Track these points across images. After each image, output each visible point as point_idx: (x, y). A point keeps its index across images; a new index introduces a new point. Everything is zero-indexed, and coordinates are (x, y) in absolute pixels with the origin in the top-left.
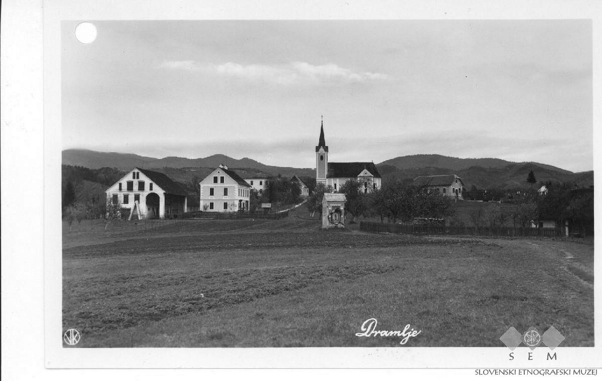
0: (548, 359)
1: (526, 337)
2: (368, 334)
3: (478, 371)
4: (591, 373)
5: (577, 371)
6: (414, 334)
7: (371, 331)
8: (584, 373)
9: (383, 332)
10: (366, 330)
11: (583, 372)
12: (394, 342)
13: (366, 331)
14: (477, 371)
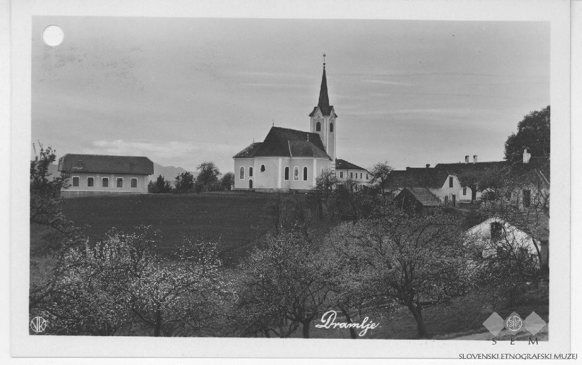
0: (529, 344)
2: (327, 326)
3: (462, 356)
4: (571, 357)
5: (557, 356)
6: (373, 326)
7: (330, 323)
8: (564, 357)
9: (342, 324)
10: (326, 322)
11: (564, 357)
12: (353, 334)
13: (325, 323)
14: (461, 355)
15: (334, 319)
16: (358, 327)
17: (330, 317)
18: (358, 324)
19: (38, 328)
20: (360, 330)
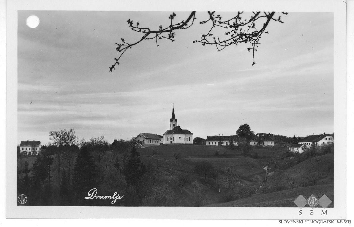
0: (322, 214)
1: (315, 199)
2: (92, 198)
3: (281, 221)
4: (347, 222)
5: (339, 221)
6: (120, 198)
7: (94, 195)
8: (343, 222)
9: (101, 196)
10: (91, 195)
11: (343, 222)
12: (107, 203)
13: (90, 197)
14: (280, 221)
15: (96, 193)
16: (111, 198)
17: (94, 191)
18: (111, 196)
19: (22, 202)
20: (112, 200)
